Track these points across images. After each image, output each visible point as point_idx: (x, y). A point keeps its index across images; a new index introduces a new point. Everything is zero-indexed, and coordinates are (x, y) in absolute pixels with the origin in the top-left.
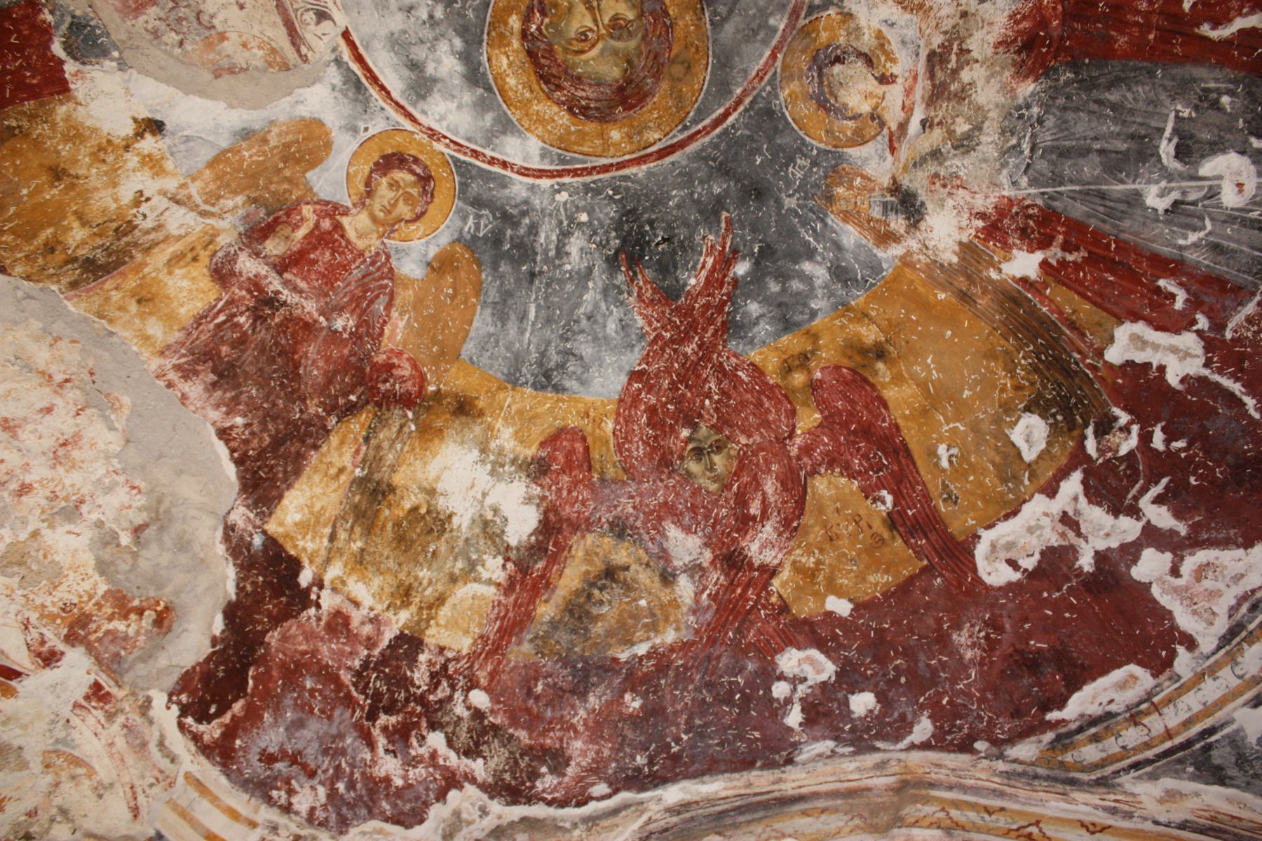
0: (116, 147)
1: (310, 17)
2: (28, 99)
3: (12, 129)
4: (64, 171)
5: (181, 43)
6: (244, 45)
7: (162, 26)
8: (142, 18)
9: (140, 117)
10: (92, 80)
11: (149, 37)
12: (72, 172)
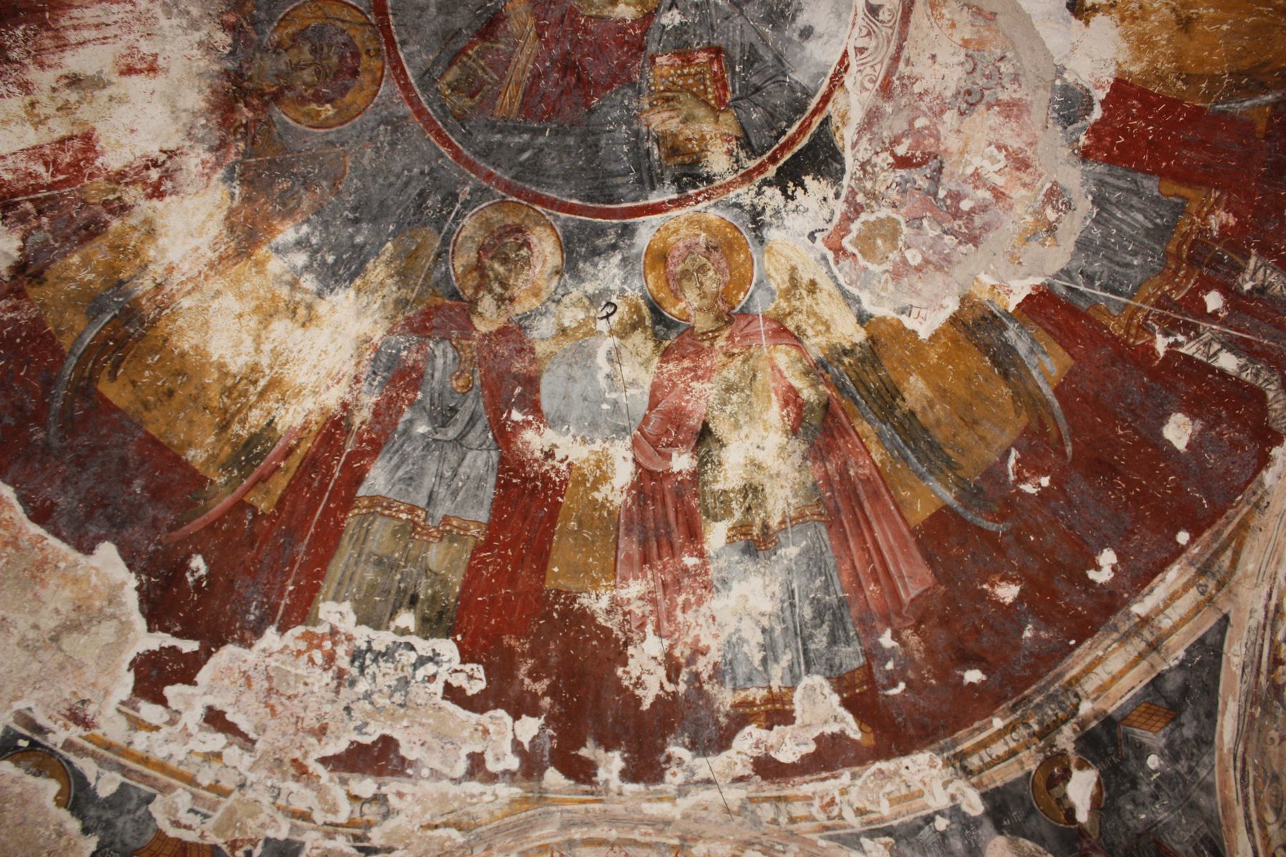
0: (1121, 12)
1: (884, 15)
2: (1152, 93)
3: (1185, 82)
4: (1179, 21)
5: (1002, 59)
6: (953, 26)
7: (1006, 81)
8: (1016, 96)
9: (1081, 23)
10: (1092, 75)
11: (1022, 79)
12: (1173, 17)
